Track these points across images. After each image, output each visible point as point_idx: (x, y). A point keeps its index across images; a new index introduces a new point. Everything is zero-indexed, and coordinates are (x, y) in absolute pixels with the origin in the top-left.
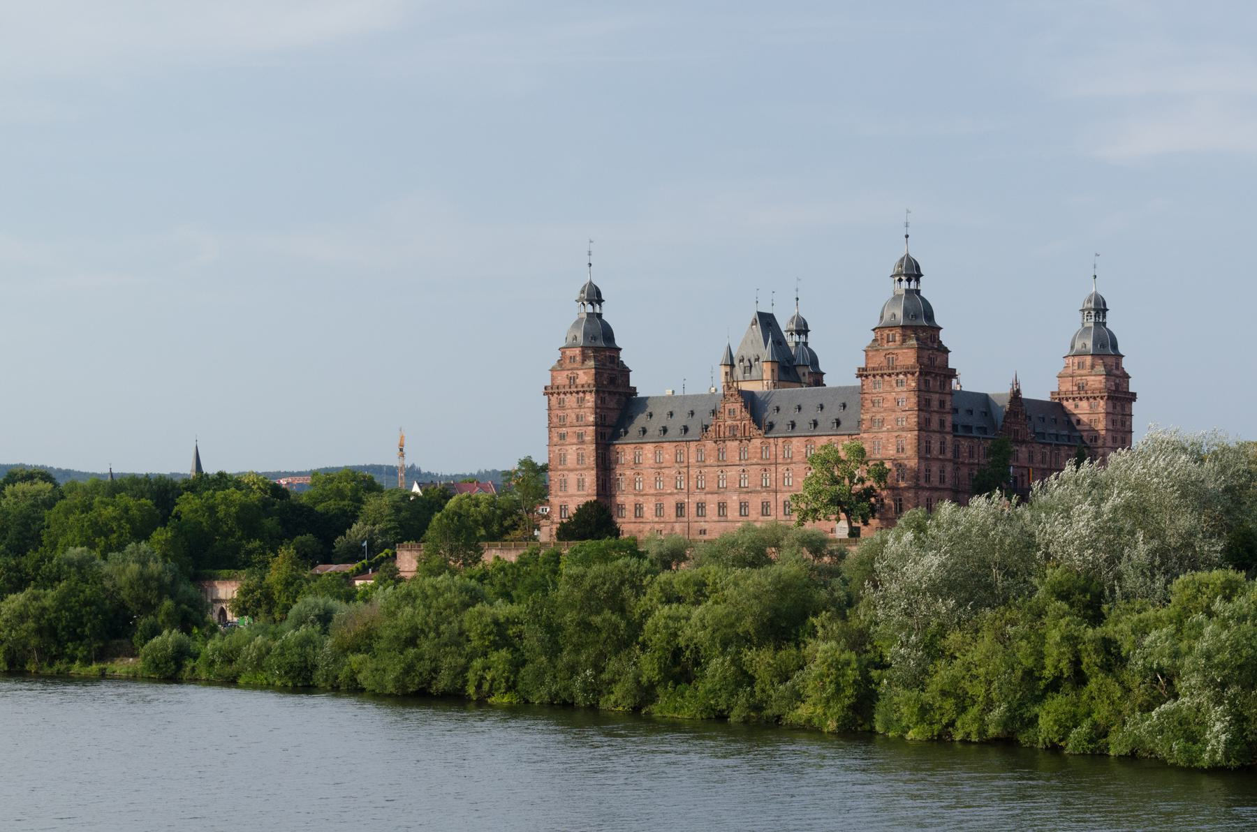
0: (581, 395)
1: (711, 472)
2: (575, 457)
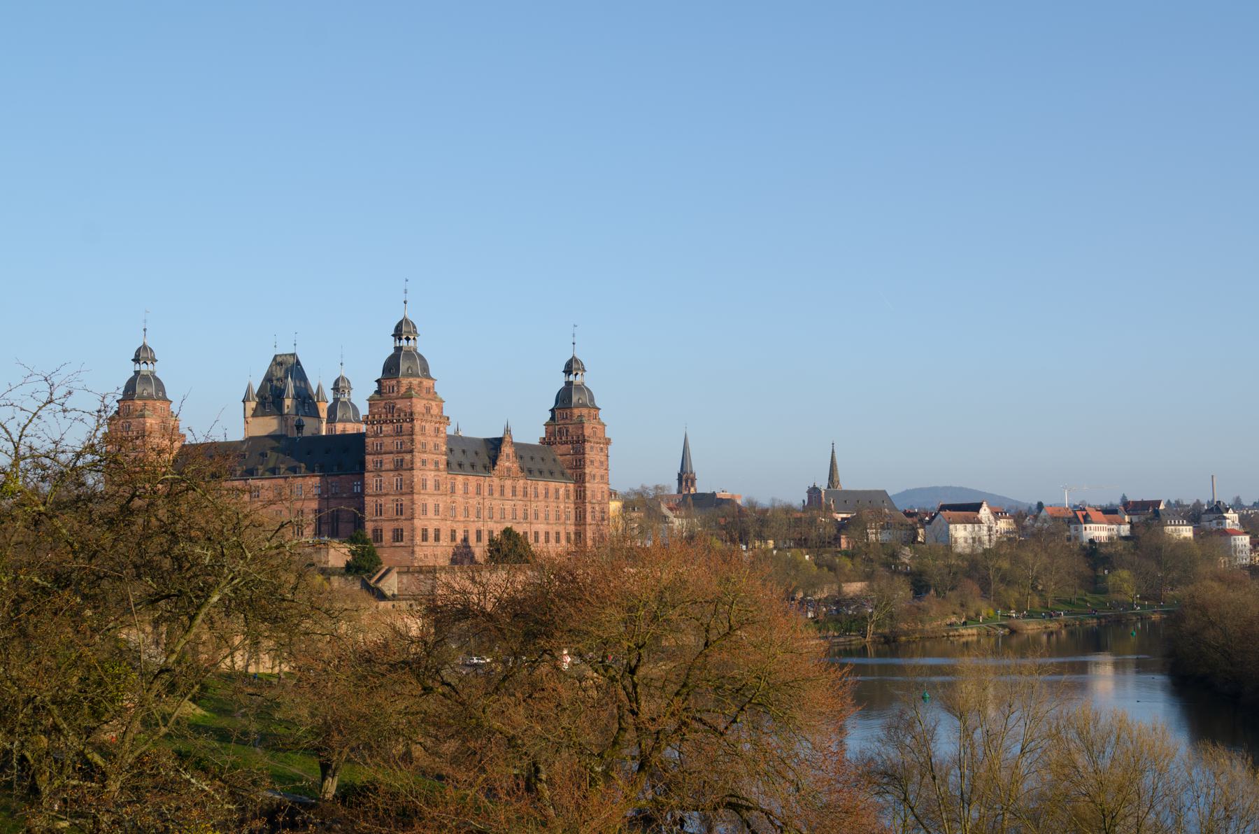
0: (437, 425)
1: (497, 503)
2: (433, 483)
